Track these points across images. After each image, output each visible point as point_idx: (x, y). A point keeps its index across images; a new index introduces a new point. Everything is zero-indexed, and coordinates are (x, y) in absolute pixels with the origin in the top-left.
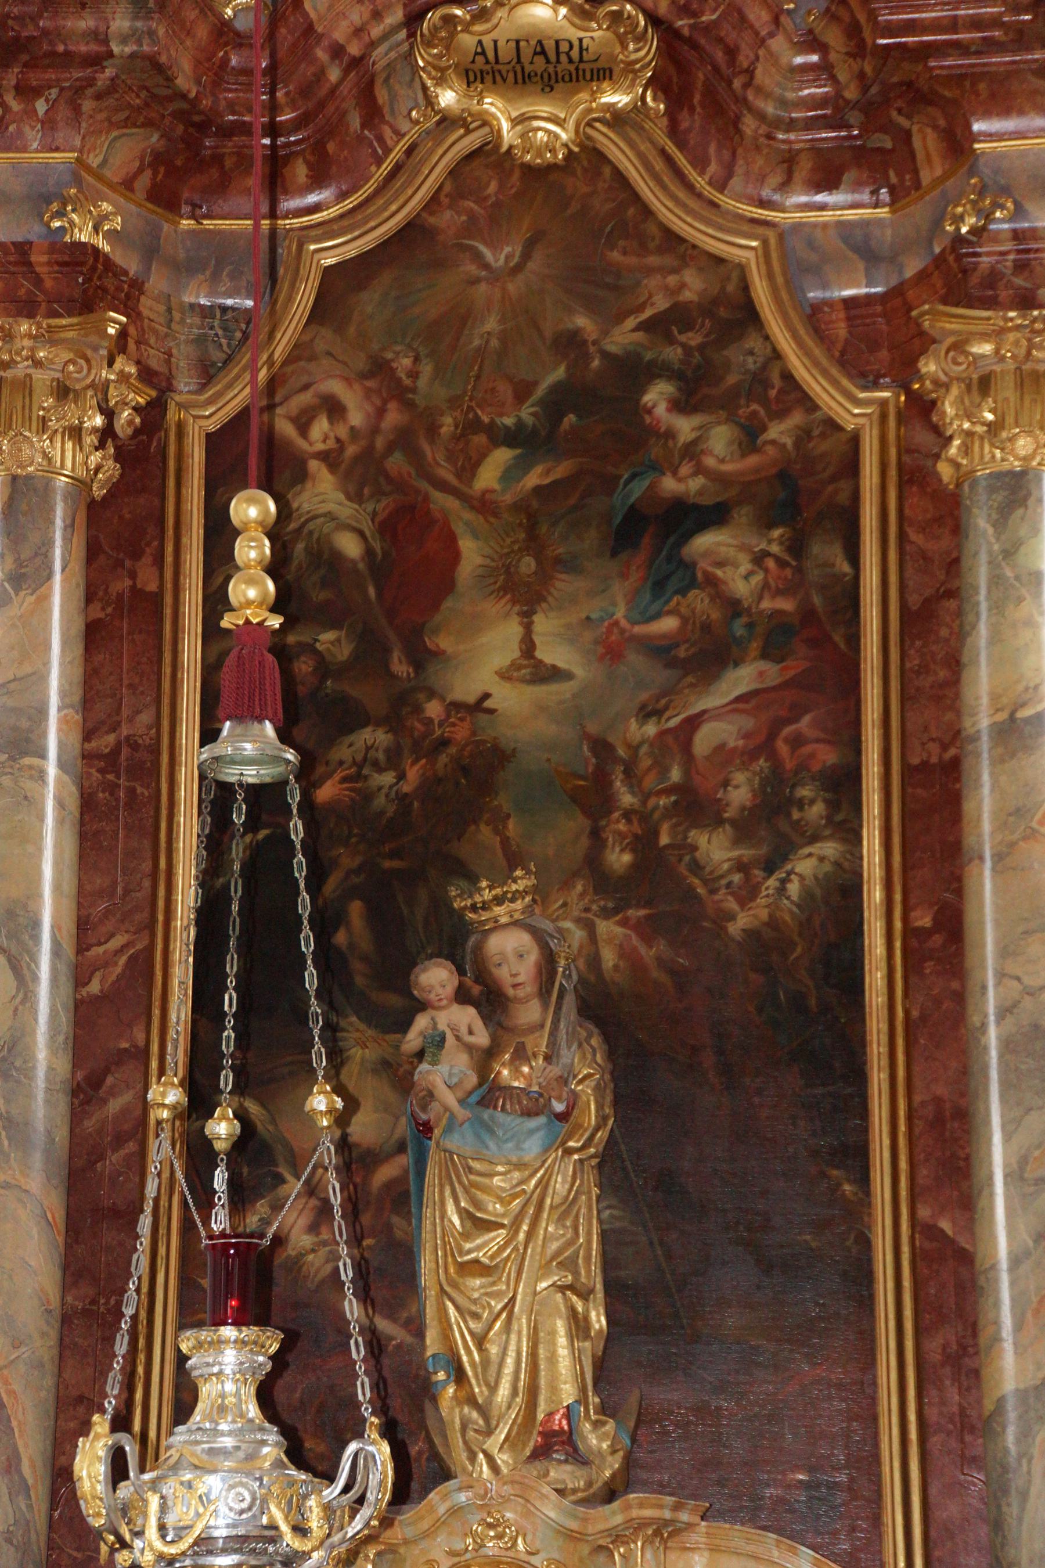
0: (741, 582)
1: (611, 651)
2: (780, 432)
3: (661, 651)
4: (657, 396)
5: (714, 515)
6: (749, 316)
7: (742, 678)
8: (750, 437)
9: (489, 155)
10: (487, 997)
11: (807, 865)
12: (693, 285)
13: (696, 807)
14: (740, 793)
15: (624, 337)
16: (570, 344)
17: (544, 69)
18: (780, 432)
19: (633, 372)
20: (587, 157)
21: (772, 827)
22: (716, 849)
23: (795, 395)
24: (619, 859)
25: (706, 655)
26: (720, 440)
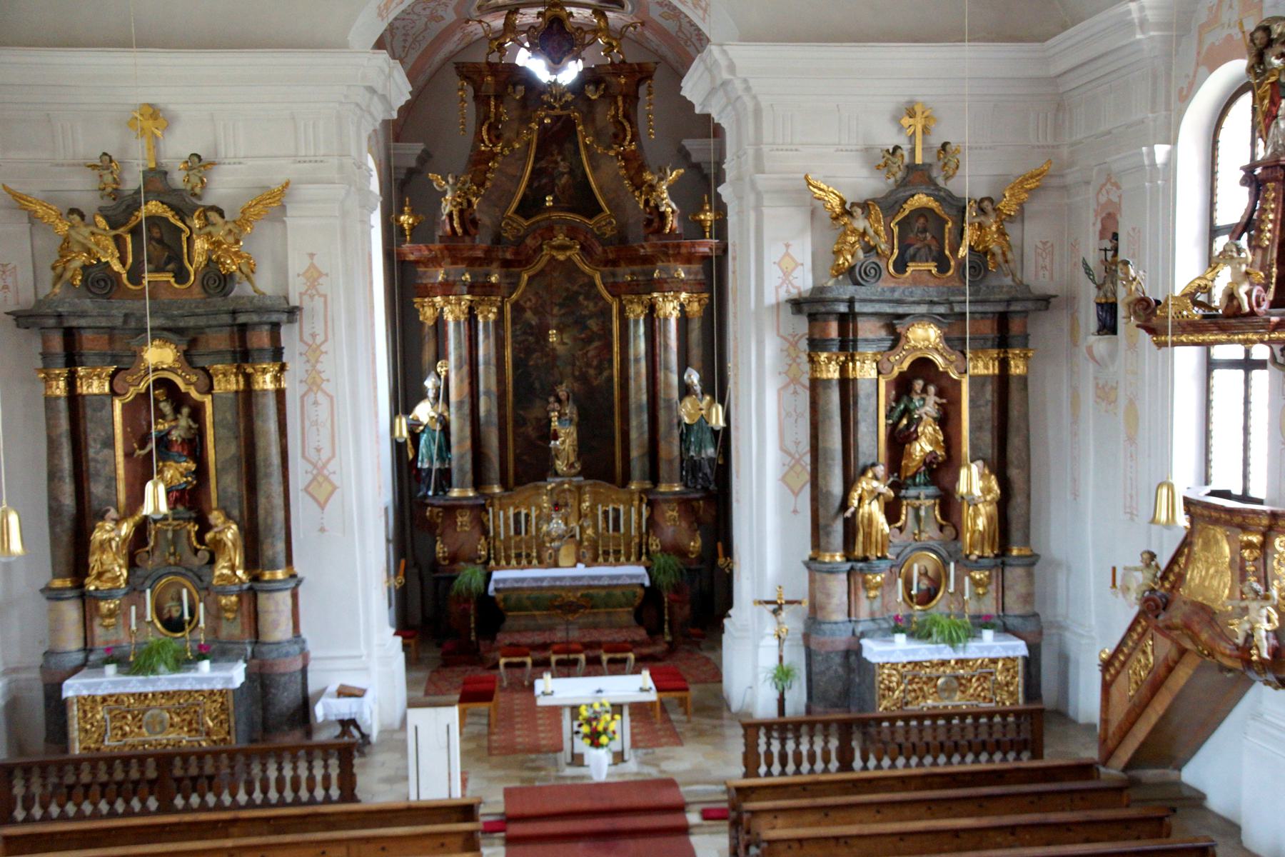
0: (595, 328)
1: (575, 339)
2: (601, 304)
3: (583, 340)
4: (581, 298)
5: (591, 317)
6: (593, 285)
7: (596, 344)
8: (596, 304)
9: (553, 257)
10: (559, 400)
11: (606, 374)
12: (586, 280)
13: (588, 365)
14: (595, 363)
15: (575, 288)
16: (567, 290)
17: (562, 248)
18: (601, 304)
19: (578, 293)
20: (569, 259)
21: (600, 369)
22: (592, 372)
23: (602, 298)
24: (577, 373)
25: (589, 341)
26: (591, 306)
